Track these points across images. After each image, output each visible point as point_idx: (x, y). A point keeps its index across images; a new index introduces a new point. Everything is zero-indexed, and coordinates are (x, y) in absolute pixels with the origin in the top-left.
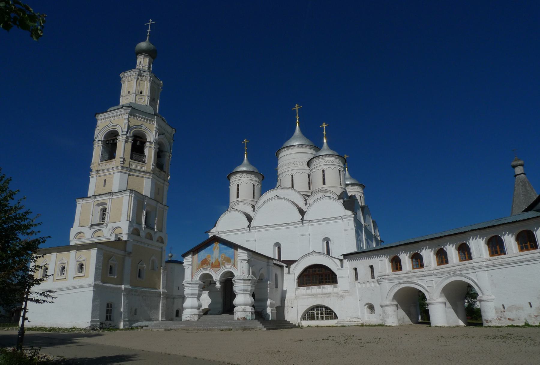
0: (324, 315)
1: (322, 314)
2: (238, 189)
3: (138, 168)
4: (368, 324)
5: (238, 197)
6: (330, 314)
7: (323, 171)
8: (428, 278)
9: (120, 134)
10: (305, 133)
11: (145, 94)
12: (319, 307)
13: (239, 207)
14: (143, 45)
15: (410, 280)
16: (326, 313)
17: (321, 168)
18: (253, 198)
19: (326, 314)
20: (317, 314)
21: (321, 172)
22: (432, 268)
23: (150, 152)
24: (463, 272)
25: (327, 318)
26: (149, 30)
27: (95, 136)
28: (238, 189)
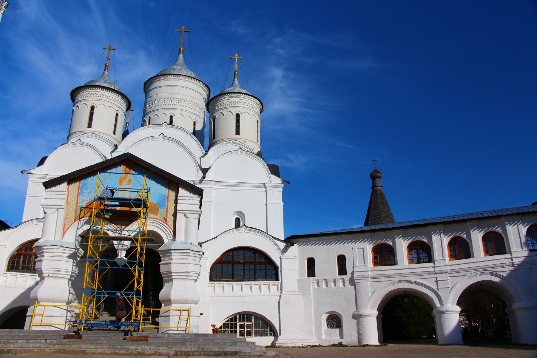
0: (253, 330)
1: (249, 326)
2: (91, 114)
4: (352, 345)
5: (90, 125)
6: (266, 327)
7: (238, 116)
8: (440, 277)
12: (245, 316)
15: (410, 279)
16: (256, 325)
17: (235, 111)
19: (255, 327)
20: (242, 327)
21: (235, 117)
24: (497, 270)
25: (257, 334)
28: (91, 114)
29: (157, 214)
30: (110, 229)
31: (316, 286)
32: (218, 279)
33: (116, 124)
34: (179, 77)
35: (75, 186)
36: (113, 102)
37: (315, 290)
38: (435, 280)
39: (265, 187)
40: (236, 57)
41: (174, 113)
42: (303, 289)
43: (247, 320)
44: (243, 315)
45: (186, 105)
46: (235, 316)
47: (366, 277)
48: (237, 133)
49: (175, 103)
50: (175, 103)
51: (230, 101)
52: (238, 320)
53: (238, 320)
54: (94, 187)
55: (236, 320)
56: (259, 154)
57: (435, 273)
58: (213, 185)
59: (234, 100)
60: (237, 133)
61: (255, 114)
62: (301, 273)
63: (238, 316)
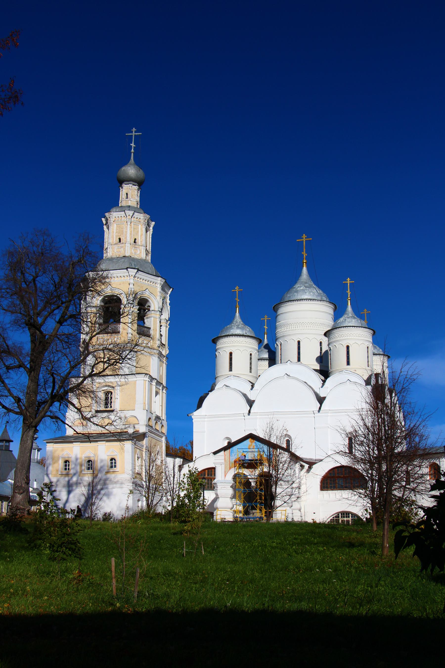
5: (231, 370)
9: (124, 301)
10: (317, 280)
11: (140, 244)
13: (233, 382)
18: (251, 372)
26: (133, 145)
30: (246, 472)
33: (251, 363)
34: (302, 302)
35: (228, 452)
40: (348, 282)
41: (300, 338)
43: (346, 517)
44: (344, 514)
46: (338, 513)
48: (348, 363)
49: (301, 328)
50: (301, 328)
51: (340, 334)
52: (340, 517)
53: (340, 517)
54: (237, 452)
55: (339, 517)
56: (365, 381)
60: (348, 363)
61: (364, 342)
63: (340, 514)
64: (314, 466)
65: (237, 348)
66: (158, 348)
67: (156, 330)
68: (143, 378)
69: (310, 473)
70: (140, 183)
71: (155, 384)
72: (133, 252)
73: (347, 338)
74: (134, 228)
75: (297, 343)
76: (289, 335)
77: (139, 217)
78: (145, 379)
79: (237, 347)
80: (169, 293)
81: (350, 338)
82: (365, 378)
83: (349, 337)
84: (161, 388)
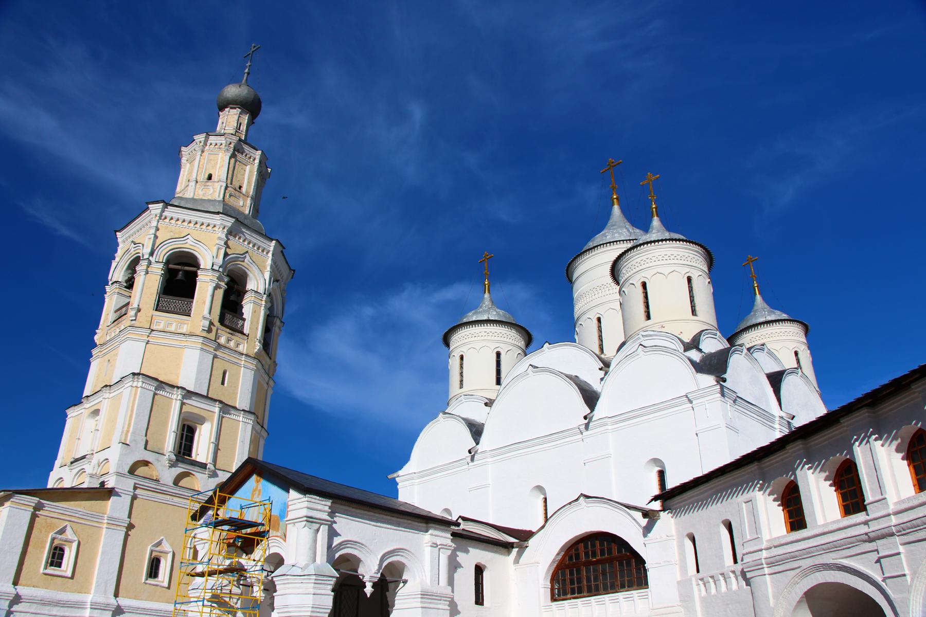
3: (173, 328)
8: (884, 547)
14: (232, 91)
15: (829, 559)
21: (640, 289)
22: (892, 508)
23: (207, 291)
27: (110, 278)
29: (278, 530)
31: (703, 593)
32: (569, 596)
34: (597, 251)
36: (489, 338)
37: (703, 600)
38: (875, 556)
39: (691, 402)
41: (600, 311)
42: (686, 599)
45: (607, 292)
47: (758, 566)
48: (648, 317)
57: (871, 540)
58: (606, 425)
59: (634, 263)
62: (683, 569)
64: (532, 542)
65: (469, 346)
66: (205, 334)
67: (204, 303)
68: (130, 384)
69: (411, 550)
70: (252, 107)
71: (180, 397)
72: (201, 192)
73: (641, 268)
74: (209, 160)
75: (595, 321)
76: (584, 313)
77: (219, 142)
78: (135, 384)
79: (479, 346)
80: (272, 249)
81: (647, 265)
82: (687, 339)
83: (644, 267)
84: (217, 410)
